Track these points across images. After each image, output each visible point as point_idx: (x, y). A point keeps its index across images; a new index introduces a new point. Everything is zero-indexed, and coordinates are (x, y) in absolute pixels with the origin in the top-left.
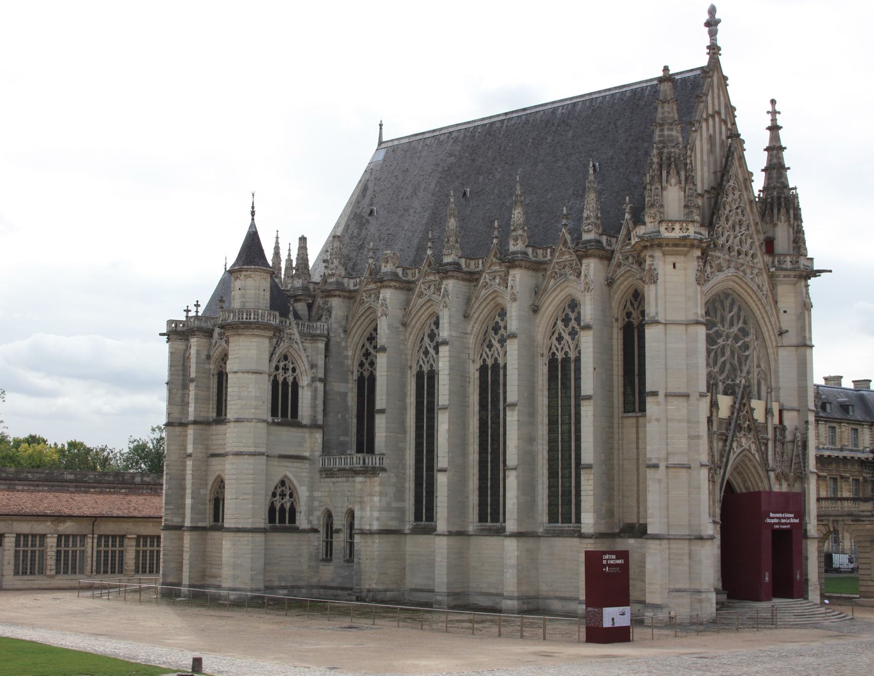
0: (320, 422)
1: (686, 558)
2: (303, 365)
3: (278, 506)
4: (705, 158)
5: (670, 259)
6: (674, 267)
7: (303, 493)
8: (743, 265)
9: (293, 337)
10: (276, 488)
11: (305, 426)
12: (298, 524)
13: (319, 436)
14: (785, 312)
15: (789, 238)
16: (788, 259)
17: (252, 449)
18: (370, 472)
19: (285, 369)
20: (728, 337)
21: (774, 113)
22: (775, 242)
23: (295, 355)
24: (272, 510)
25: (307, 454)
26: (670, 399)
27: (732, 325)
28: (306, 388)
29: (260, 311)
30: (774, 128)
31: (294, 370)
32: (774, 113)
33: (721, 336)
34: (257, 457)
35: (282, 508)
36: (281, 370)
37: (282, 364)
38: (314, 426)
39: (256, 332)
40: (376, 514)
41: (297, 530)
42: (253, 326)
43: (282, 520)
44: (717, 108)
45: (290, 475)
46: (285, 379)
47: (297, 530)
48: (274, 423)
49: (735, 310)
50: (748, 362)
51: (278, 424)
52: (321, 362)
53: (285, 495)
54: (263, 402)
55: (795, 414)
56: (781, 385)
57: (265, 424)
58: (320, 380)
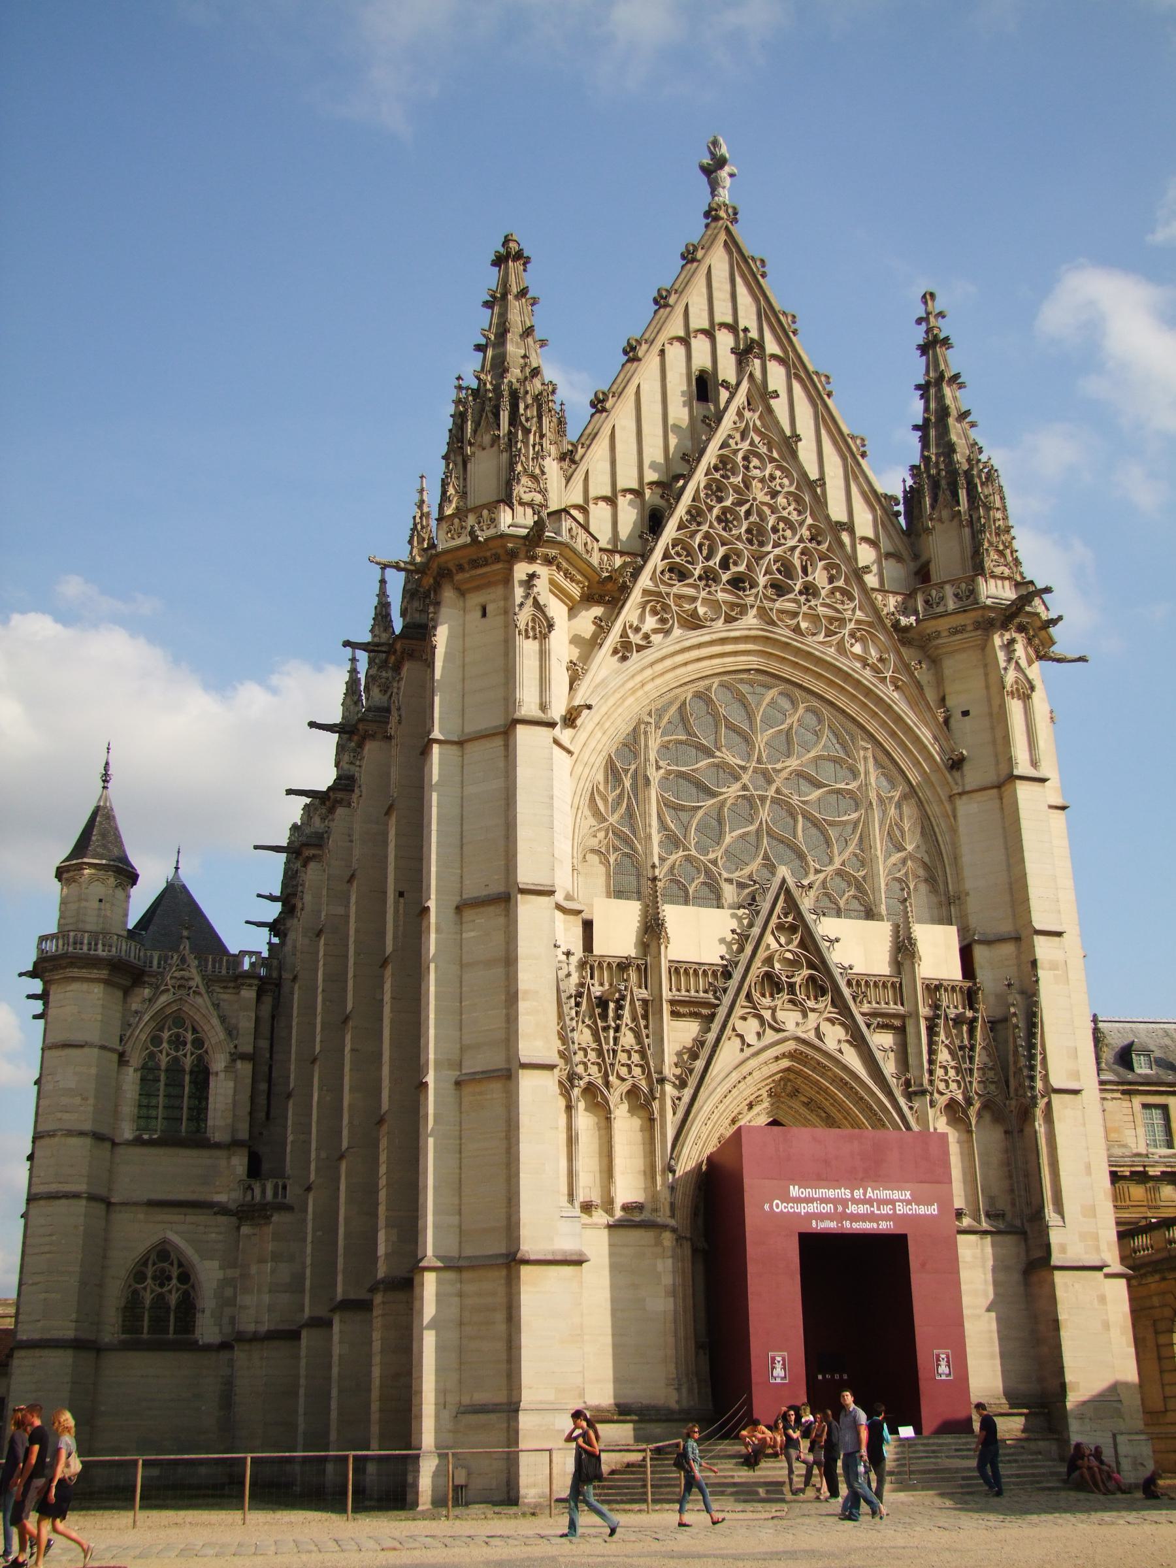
0: (243, 1135)
1: (500, 1316)
2: (215, 1033)
3: (148, 1298)
6: (484, 615)
7: (209, 1273)
8: (795, 615)
9: (191, 983)
10: (144, 1262)
11: (218, 1146)
12: (198, 1335)
13: (239, 1163)
14: (966, 713)
15: (962, 551)
16: (949, 590)
17: (53, 1188)
18: (249, 1213)
19: (177, 1042)
22: (932, 567)
24: (131, 1308)
25: (222, 1198)
26: (468, 914)
28: (222, 1075)
29: (72, 934)
31: (199, 1043)
33: (737, 778)
34: (63, 1201)
37: (166, 1035)
38: (235, 1144)
39: (76, 972)
40: (266, 1298)
41: (194, 1347)
42: (64, 962)
43: (159, 1324)
46: (176, 1060)
47: (194, 1347)
48: (138, 1142)
51: (151, 1143)
52: (246, 1023)
53: (169, 1278)
54: (85, 1099)
55: (1008, 949)
56: (969, 885)
57: (88, 1141)
58: (243, 1057)
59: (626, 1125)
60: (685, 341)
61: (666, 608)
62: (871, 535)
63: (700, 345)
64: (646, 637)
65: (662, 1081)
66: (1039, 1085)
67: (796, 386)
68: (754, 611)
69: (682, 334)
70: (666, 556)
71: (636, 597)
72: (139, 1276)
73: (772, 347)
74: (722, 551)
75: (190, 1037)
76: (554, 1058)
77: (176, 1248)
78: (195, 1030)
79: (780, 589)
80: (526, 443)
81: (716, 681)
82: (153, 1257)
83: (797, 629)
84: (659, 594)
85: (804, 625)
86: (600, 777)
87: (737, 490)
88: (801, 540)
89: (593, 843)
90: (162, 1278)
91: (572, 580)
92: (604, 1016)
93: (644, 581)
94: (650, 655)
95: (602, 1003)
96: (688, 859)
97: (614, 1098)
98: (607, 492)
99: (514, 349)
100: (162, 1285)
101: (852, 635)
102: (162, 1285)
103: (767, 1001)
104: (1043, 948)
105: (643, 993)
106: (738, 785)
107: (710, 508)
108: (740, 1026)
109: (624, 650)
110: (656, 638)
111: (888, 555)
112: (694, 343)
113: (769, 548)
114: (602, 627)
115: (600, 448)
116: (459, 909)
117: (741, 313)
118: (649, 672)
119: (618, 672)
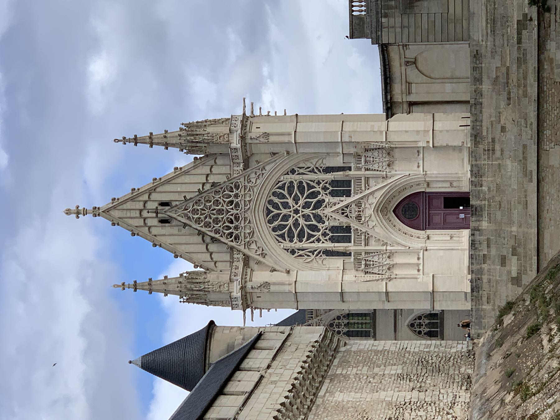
4: (175, 231)
5: (255, 299)
20: (296, 212)
21: (125, 140)
23: (329, 319)
26: (344, 300)
27: (286, 205)
30: (136, 140)
32: (125, 140)
35: (428, 325)
36: (340, 329)
37: (336, 330)
44: (138, 212)
45: (407, 322)
49: (276, 200)
50: (312, 183)
53: (420, 323)
59: (398, 260)
60: (149, 228)
61: (248, 242)
62: (209, 168)
63: (150, 222)
64: (258, 248)
65: (386, 250)
66: (384, 145)
67: (158, 190)
68: (246, 214)
69: (147, 228)
70: (232, 241)
71: (246, 251)
72: (420, 333)
73: (145, 197)
74: (227, 224)
75: (337, 321)
76: (384, 283)
77: (409, 322)
78: (334, 319)
79: (237, 205)
80: (208, 288)
81: (268, 224)
82: (413, 329)
83: (250, 201)
84: (245, 244)
85: (248, 199)
86: (301, 260)
87: (206, 218)
88: (220, 198)
89: (320, 262)
90: (420, 325)
91: (246, 272)
92: (370, 265)
93: (242, 248)
94: (265, 247)
95: (366, 265)
96: (323, 235)
97: (391, 263)
98: (208, 255)
99: (171, 288)
100: (422, 325)
101: (248, 183)
102: (422, 325)
103: (363, 219)
104: (346, 139)
105: (363, 254)
106: (298, 218)
107: (214, 227)
108: (370, 227)
109: (264, 255)
110: (258, 245)
111: (215, 162)
112: (149, 224)
113: (224, 208)
114: (258, 263)
115: (195, 256)
116: (343, 302)
117: (134, 208)
118: (269, 247)
119: (271, 257)
